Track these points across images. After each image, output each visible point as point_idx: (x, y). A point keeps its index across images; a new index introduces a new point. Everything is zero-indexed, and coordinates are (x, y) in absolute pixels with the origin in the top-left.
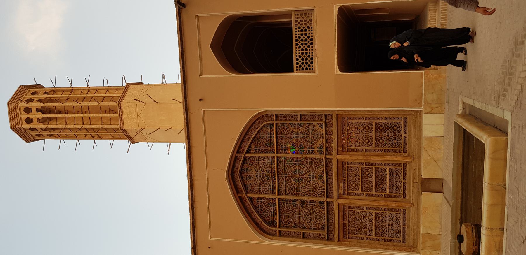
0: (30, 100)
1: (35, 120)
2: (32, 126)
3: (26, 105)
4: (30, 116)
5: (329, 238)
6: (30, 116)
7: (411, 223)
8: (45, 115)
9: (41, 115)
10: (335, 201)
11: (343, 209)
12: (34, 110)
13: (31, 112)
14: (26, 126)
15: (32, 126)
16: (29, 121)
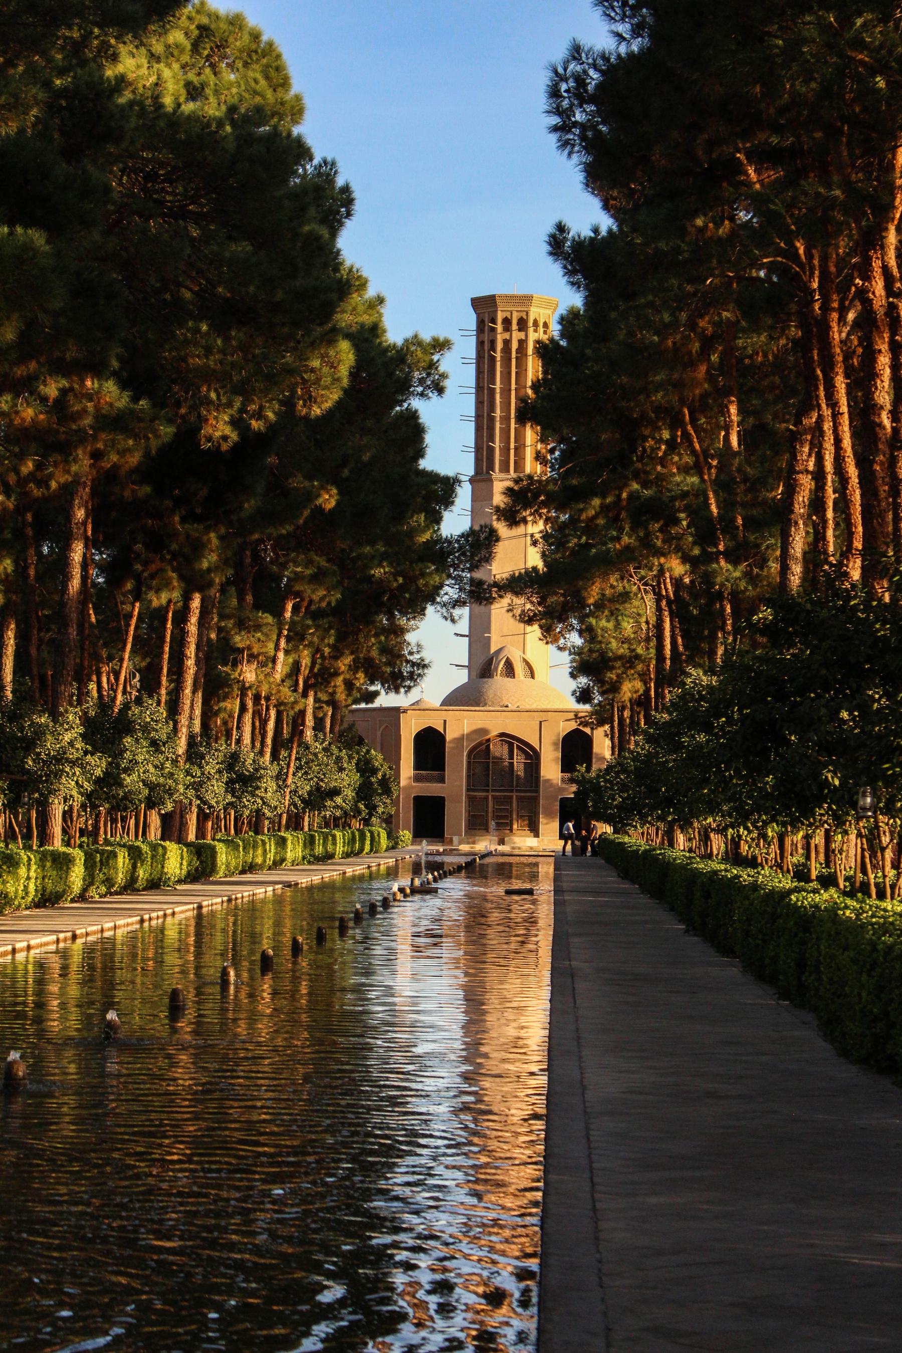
0: (536, 323)
1: (507, 336)
2: (499, 327)
3: (531, 323)
4: (515, 326)
5: (468, 790)
6: (515, 326)
7: (478, 832)
8: (514, 355)
9: (515, 345)
10: (490, 795)
11: (487, 798)
12: (522, 335)
13: (520, 330)
14: (500, 316)
15: (499, 327)
16: (507, 322)
